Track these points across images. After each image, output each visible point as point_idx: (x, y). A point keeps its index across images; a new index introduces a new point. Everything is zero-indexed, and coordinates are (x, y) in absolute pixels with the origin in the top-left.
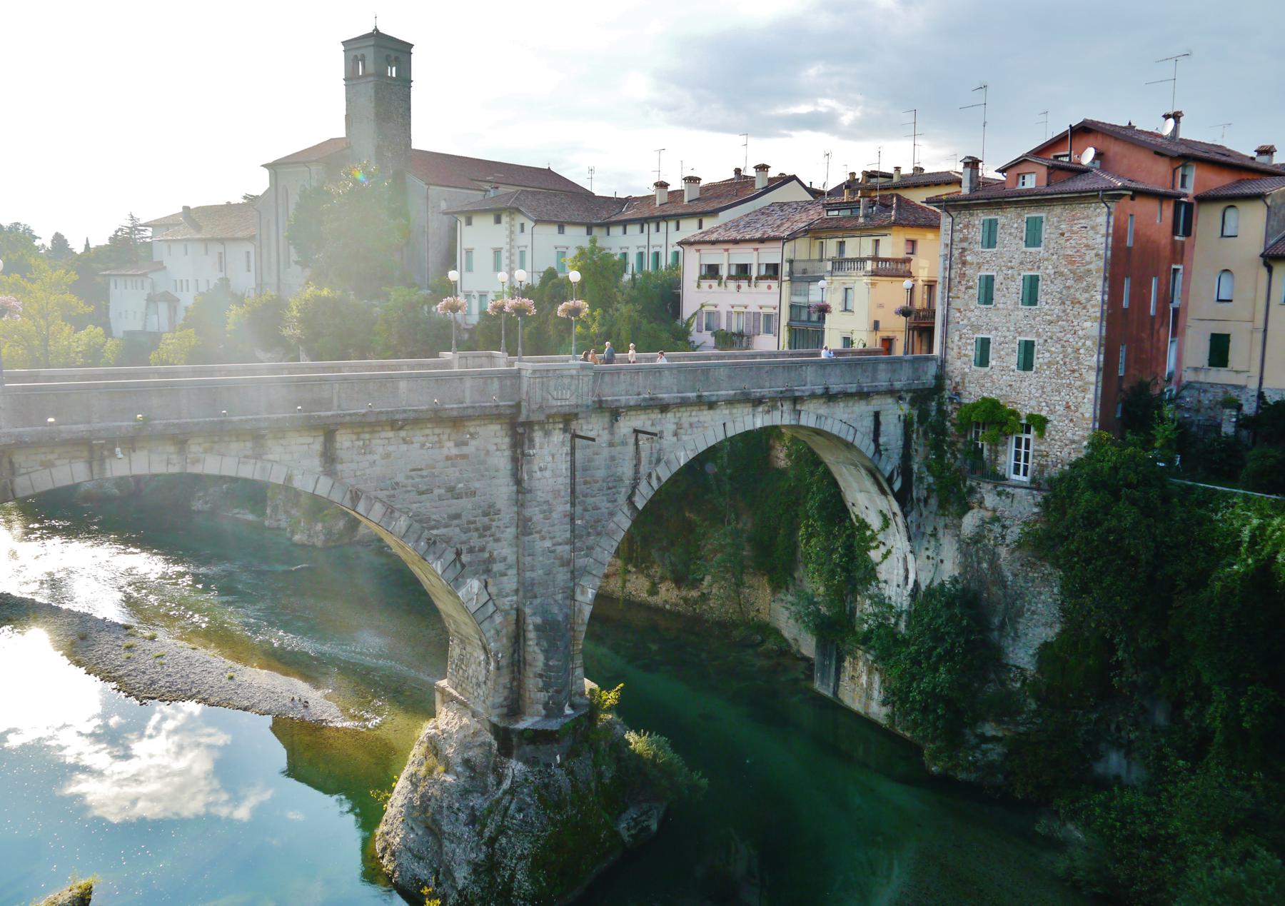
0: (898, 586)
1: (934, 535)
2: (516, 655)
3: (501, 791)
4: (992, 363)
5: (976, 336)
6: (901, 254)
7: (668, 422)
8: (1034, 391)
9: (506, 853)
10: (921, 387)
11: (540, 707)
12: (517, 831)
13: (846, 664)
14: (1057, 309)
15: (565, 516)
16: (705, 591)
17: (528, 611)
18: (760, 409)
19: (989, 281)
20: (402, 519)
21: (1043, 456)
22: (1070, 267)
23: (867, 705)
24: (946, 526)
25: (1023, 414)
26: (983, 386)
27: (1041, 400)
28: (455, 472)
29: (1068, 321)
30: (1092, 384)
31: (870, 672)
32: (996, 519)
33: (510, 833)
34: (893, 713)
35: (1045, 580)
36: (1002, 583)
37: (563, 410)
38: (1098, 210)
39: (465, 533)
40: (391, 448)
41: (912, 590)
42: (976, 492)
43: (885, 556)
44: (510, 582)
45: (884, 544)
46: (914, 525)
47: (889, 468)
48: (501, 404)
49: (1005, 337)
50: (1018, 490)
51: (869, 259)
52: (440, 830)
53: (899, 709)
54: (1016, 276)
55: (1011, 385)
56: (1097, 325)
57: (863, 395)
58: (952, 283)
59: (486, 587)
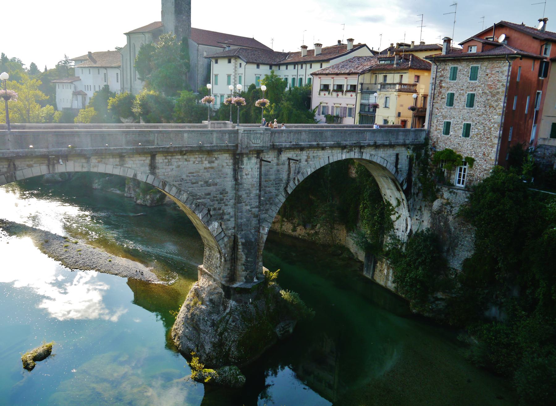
0: (403, 231)
1: (420, 209)
2: (233, 256)
3: (226, 313)
4: (451, 133)
5: (444, 120)
6: (412, 81)
7: (303, 155)
8: (469, 146)
9: (227, 339)
10: (418, 143)
11: (243, 278)
12: (232, 330)
13: (378, 265)
14: (483, 109)
15: (256, 196)
16: (317, 231)
17: (239, 236)
18: (345, 151)
19: (452, 95)
20: (185, 194)
21: (471, 176)
22: (490, 90)
23: (386, 283)
24: (426, 206)
25: (463, 157)
26: (446, 144)
27: (472, 151)
28: (208, 175)
29: (487, 115)
30: (496, 144)
31: (388, 269)
32: (448, 203)
33: (229, 331)
34: (398, 286)
35: (468, 231)
36: (449, 231)
37: (257, 148)
38: (505, 64)
39: (212, 201)
40: (180, 163)
41: (409, 233)
42: (440, 191)
43: (398, 218)
44: (231, 224)
45: (397, 213)
46: (411, 205)
47: (402, 179)
48: (229, 145)
49: (458, 122)
50: (459, 191)
51: (397, 84)
52: (199, 328)
53: (400, 285)
54: (464, 93)
55: (459, 144)
56: (500, 117)
57: (391, 146)
58: (435, 96)
59: (221, 225)
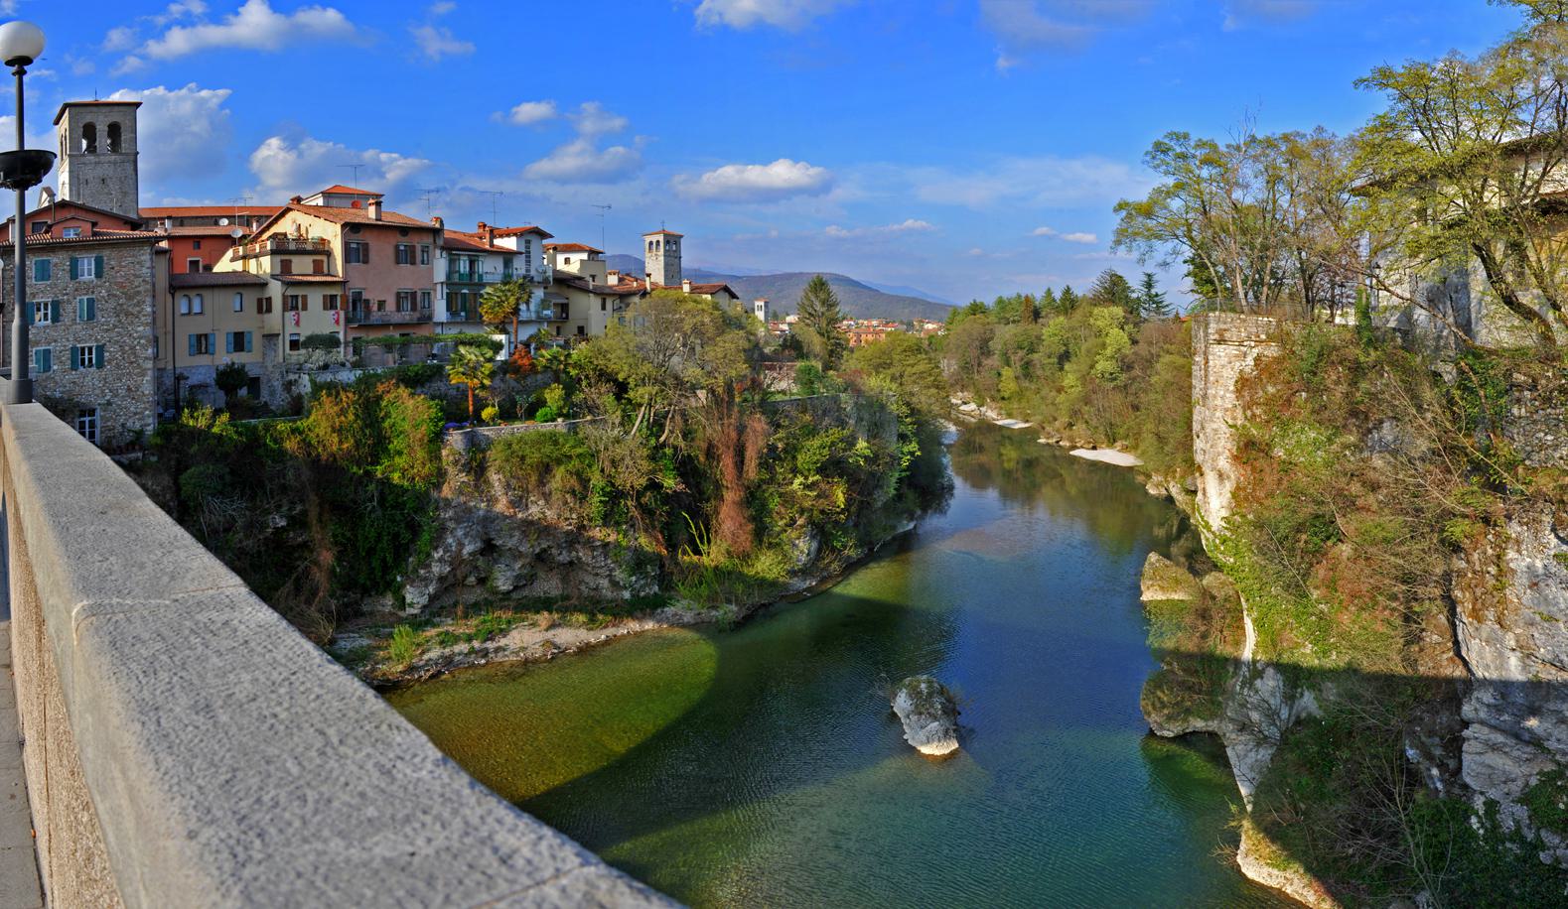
14: (113, 320)
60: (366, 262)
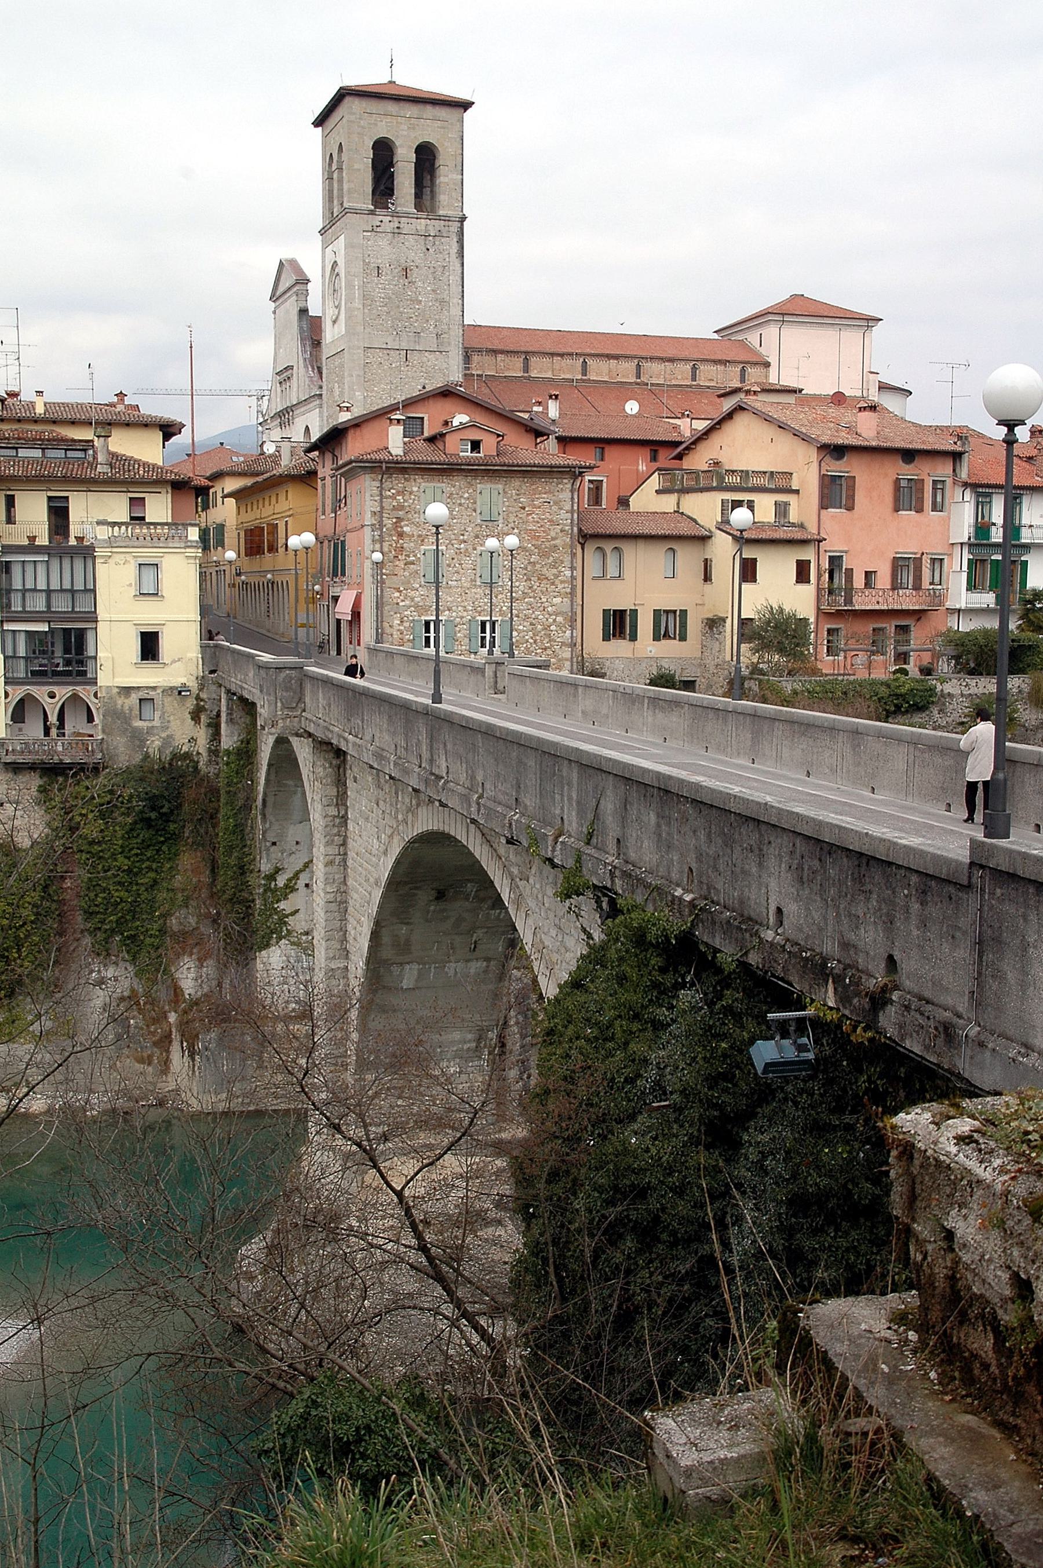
29: (535, 598)
30: (567, 660)
49: (462, 617)
60: (850, 508)
